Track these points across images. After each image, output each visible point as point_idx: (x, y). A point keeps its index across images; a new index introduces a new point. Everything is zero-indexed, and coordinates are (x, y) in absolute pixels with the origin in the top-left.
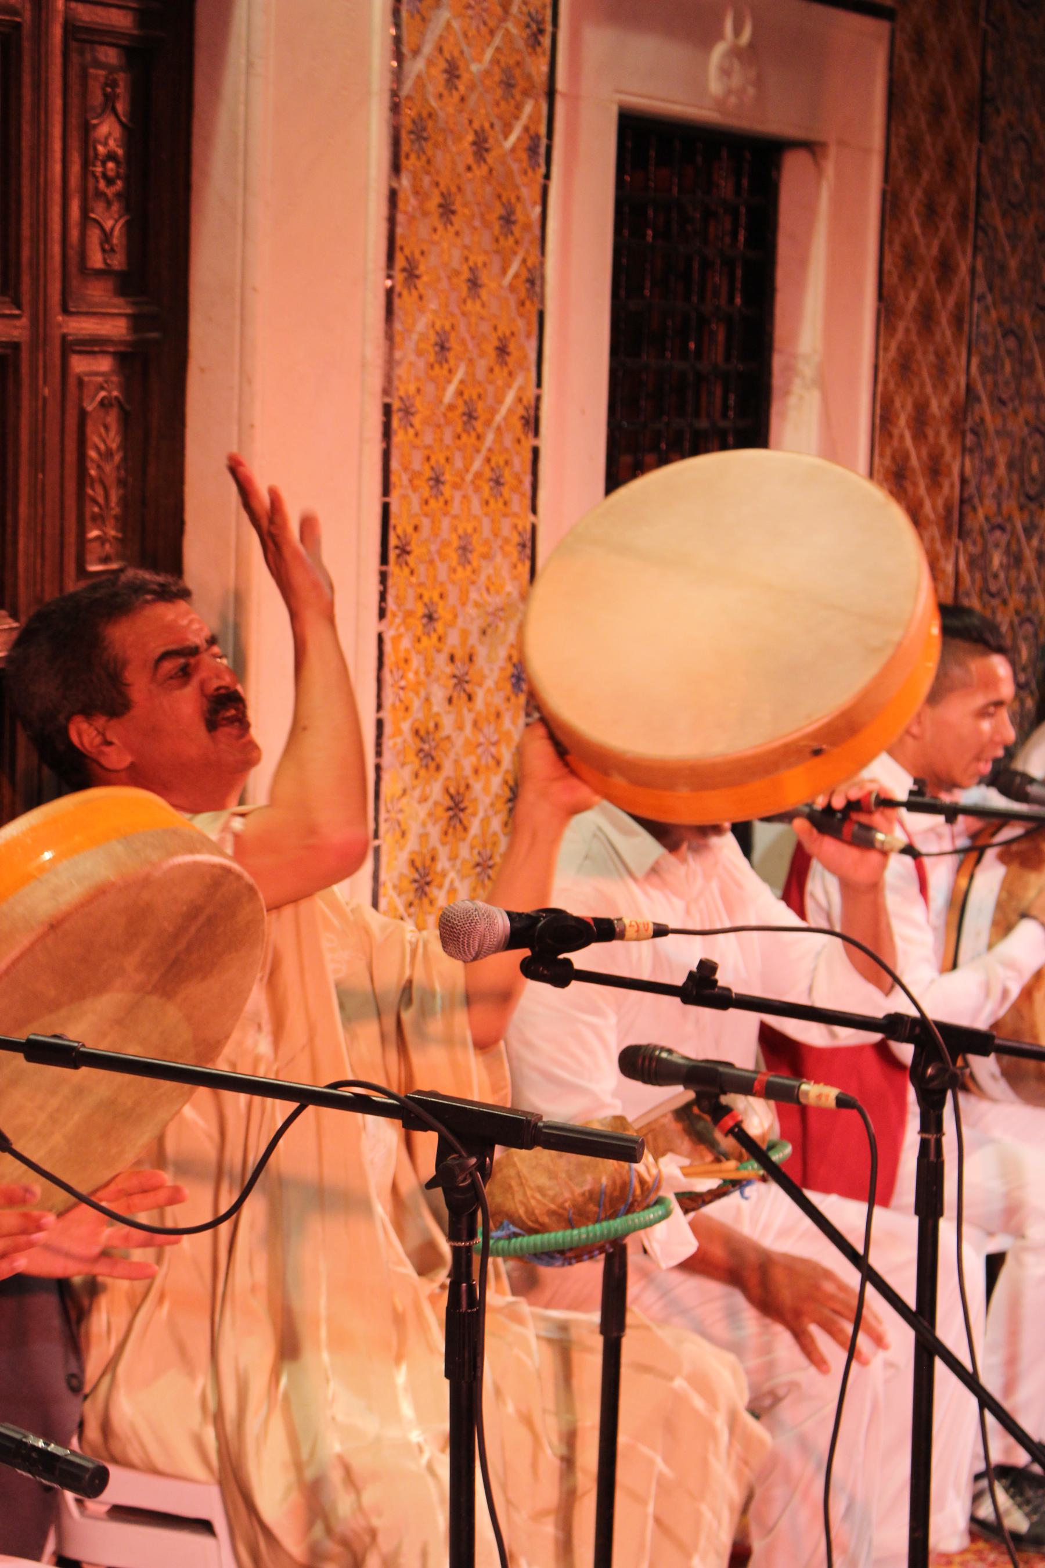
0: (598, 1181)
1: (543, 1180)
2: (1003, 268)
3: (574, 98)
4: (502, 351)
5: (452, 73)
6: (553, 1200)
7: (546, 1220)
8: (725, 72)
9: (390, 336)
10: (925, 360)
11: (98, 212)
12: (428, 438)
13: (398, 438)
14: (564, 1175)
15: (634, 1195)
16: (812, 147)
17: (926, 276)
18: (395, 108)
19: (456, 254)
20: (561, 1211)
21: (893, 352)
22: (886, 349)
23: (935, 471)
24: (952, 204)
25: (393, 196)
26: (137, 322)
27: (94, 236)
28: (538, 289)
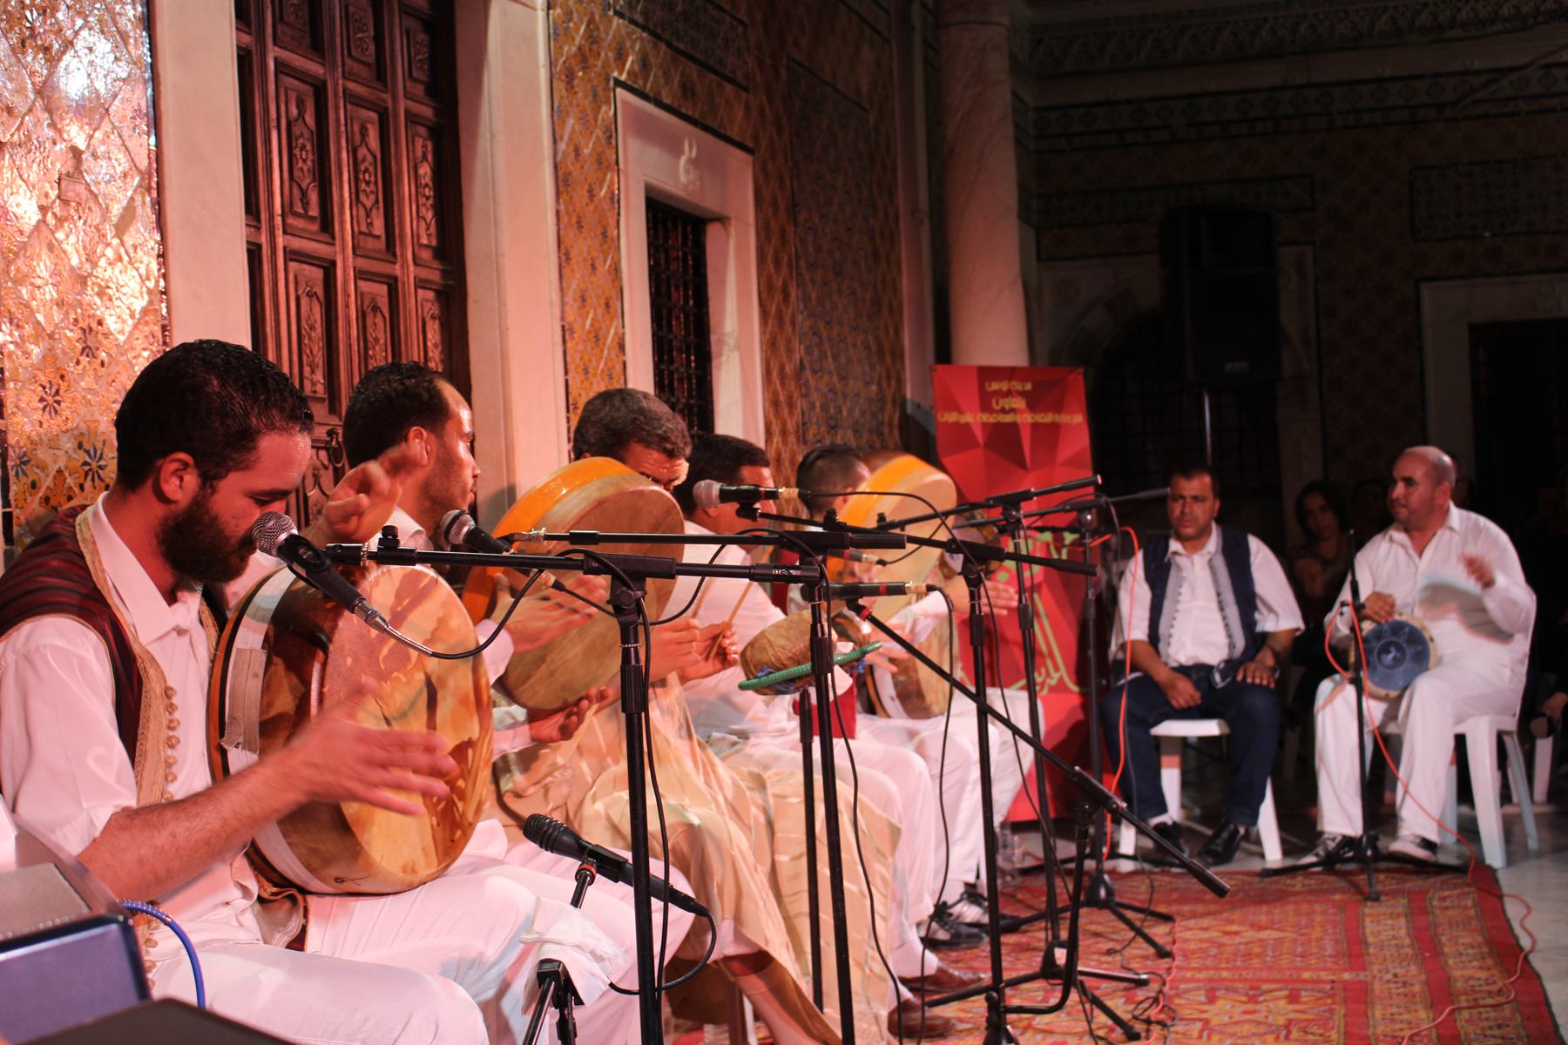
1: (783, 642)
2: (810, 298)
3: (626, 175)
4: (607, 305)
5: (577, 152)
8: (687, 172)
9: (562, 290)
10: (782, 343)
11: (423, 210)
12: (581, 347)
13: (569, 345)
16: (722, 220)
17: (778, 297)
18: (556, 166)
19: (585, 249)
23: (791, 405)
24: (785, 260)
25: (558, 213)
26: (444, 273)
27: (423, 226)
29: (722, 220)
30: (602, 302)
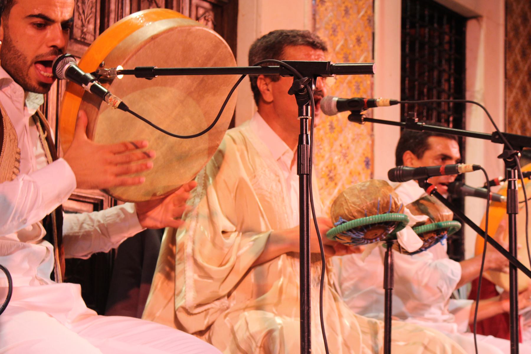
0: (376, 199)
1: (355, 200)
6: (359, 206)
7: (356, 214)
9: (314, 19)
14: (363, 197)
15: (392, 208)
16: (477, 17)
20: (362, 210)
21: (511, 99)
22: (509, 97)
28: (372, 23)
29: (477, 17)
30: (354, 37)
